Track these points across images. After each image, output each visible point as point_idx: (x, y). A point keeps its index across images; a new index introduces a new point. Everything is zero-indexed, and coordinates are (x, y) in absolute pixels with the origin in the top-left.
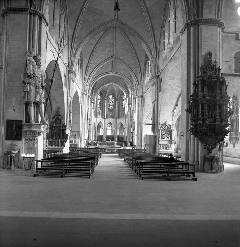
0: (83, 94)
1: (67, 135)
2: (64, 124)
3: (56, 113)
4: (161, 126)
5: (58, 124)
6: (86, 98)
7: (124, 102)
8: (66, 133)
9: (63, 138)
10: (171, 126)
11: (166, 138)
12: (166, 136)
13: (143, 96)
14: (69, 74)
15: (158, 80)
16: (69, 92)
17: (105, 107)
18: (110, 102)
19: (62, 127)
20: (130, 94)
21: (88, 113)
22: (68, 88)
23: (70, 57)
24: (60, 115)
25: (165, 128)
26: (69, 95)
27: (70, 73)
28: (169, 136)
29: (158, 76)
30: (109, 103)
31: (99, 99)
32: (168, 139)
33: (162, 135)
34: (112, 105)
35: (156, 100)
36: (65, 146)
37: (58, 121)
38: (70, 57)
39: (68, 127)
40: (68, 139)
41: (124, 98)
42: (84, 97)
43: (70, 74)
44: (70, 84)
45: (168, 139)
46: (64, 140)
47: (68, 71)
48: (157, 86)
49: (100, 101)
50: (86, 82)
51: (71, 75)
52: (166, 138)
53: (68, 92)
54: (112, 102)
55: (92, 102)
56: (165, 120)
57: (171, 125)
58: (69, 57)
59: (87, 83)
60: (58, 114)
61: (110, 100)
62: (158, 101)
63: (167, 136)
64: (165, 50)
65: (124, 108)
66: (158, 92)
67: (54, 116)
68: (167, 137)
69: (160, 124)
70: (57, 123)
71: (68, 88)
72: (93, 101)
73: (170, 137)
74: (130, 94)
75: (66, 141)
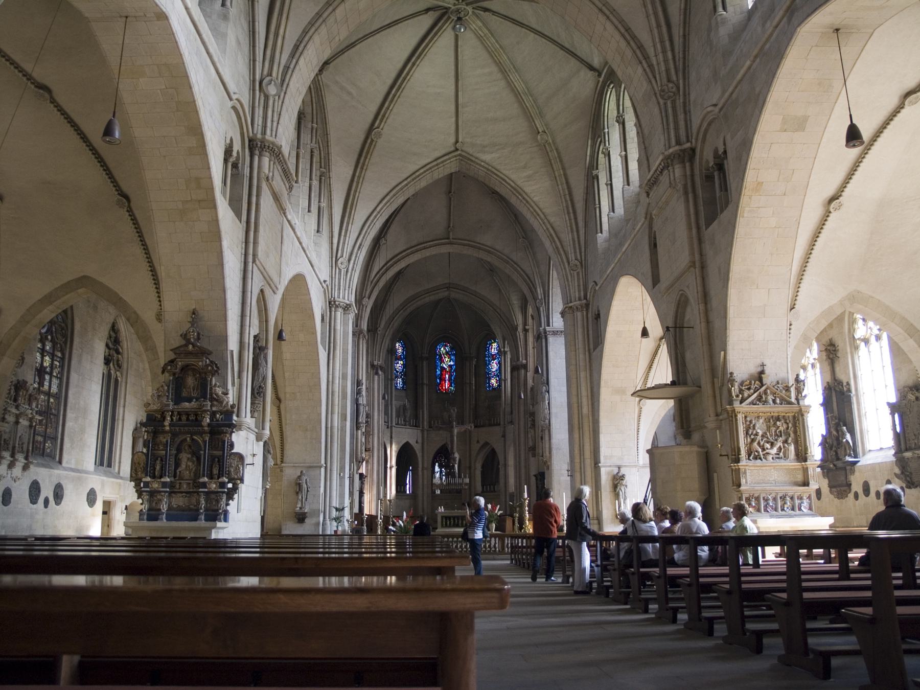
0: (332, 304)
1: (241, 457)
2: (218, 400)
3: (184, 342)
4: (741, 391)
5: (189, 400)
6: (345, 324)
7: (494, 366)
8: (232, 445)
9: (215, 471)
10: (793, 390)
11: (774, 451)
12: (772, 445)
13: (587, 305)
14: (256, 158)
15: (692, 170)
16: (255, 243)
17: (423, 384)
18: (443, 369)
19: (213, 414)
20: (520, 328)
21: (361, 402)
22: (248, 222)
23: (261, 83)
24: (203, 353)
25: (759, 398)
26: (255, 256)
27: (257, 152)
28: (786, 442)
29: (693, 150)
30: (439, 372)
31: (400, 359)
32: (786, 457)
33: (753, 441)
34: (450, 379)
35: (693, 264)
36: (226, 520)
37: (190, 381)
38: (258, 77)
39: (248, 420)
40: (242, 480)
41: (494, 351)
42: (338, 321)
43: (260, 156)
44: (258, 204)
45: (786, 457)
46: (223, 485)
47: (250, 141)
48: (691, 196)
49: (404, 365)
50: (346, 255)
51: (266, 160)
52: (774, 451)
53: (247, 242)
54: (450, 366)
55: (373, 366)
56: (759, 362)
57: (791, 381)
58: (254, 81)
59: (349, 260)
60: (188, 342)
61: (442, 361)
62: (703, 267)
63: (779, 444)
64: (729, 8)
65: (495, 385)
66: (698, 228)
67: (172, 356)
68: (780, 449)
69: (732, 381)
70: (184, 394)
71: (248, 222)
72: (375, 363)
73: (792, 448)
74: (520, 328)
75: (235, 489)
